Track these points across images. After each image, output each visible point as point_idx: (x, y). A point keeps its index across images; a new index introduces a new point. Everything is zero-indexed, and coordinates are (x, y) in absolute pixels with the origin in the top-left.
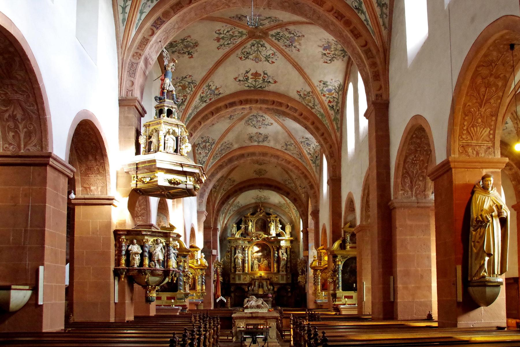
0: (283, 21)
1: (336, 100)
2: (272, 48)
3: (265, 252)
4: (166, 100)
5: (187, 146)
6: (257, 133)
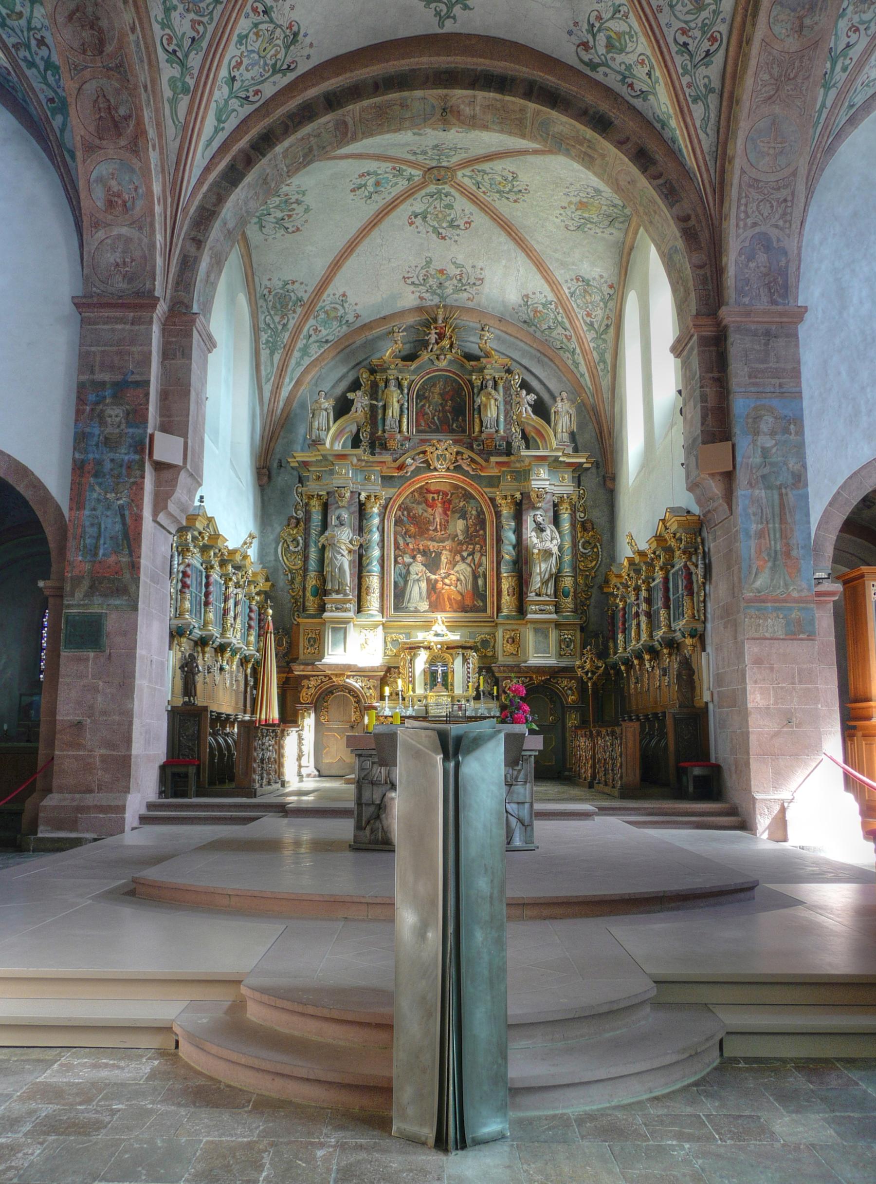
3: (460, 525)
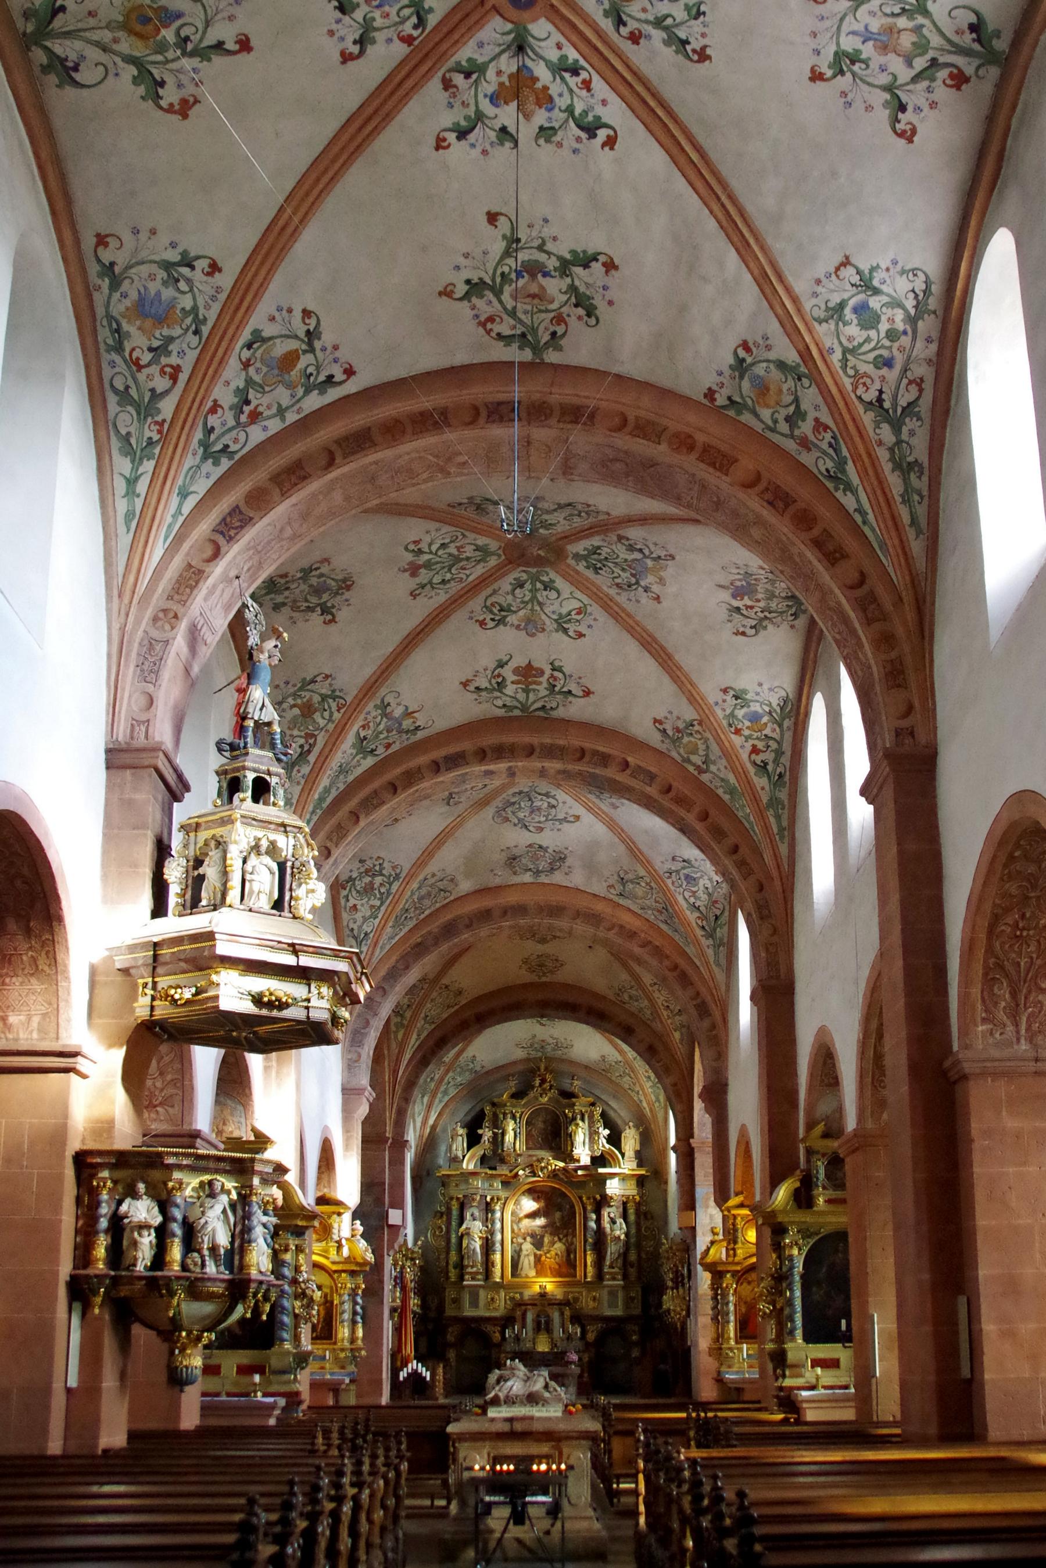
0: (608, 514)
1: (774, 745)
2: (578, 594)
3: (558, 1215)
4: (251, 750)
5: (313, 891)
6: (530, 846)
